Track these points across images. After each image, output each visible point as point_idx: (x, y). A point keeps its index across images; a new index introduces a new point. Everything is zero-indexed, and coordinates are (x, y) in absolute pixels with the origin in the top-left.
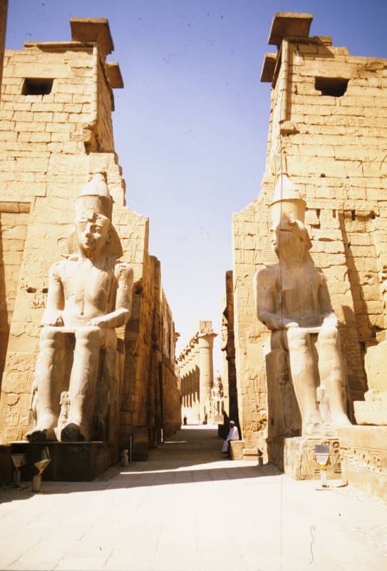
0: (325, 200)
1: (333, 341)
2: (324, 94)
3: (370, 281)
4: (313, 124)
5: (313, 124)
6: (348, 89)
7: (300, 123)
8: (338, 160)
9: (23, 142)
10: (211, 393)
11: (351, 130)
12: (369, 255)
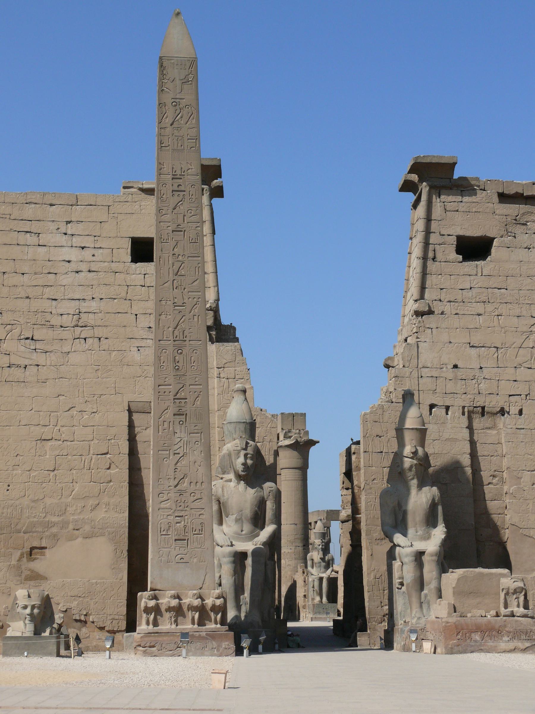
0: (455, 395)
1: (435, 558)
2: (465, 259)
3: (495, 481)
4: (450, 302)
5: (450, 302)
6: (493, 250)
7: (435, 300)
8: (473, 347)
9: (143, 328)
10: (306, 559)
11: (489, 307)
12: (495, 454)
